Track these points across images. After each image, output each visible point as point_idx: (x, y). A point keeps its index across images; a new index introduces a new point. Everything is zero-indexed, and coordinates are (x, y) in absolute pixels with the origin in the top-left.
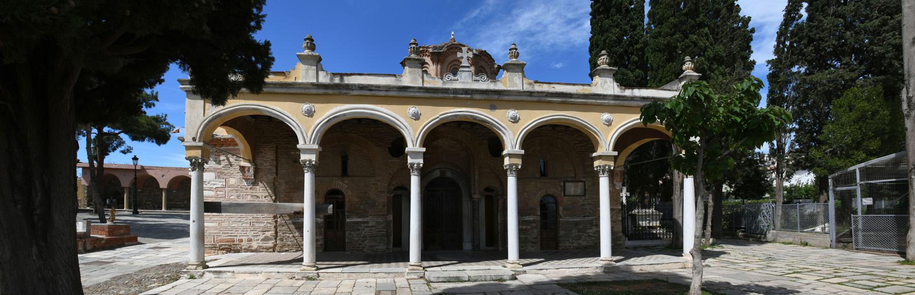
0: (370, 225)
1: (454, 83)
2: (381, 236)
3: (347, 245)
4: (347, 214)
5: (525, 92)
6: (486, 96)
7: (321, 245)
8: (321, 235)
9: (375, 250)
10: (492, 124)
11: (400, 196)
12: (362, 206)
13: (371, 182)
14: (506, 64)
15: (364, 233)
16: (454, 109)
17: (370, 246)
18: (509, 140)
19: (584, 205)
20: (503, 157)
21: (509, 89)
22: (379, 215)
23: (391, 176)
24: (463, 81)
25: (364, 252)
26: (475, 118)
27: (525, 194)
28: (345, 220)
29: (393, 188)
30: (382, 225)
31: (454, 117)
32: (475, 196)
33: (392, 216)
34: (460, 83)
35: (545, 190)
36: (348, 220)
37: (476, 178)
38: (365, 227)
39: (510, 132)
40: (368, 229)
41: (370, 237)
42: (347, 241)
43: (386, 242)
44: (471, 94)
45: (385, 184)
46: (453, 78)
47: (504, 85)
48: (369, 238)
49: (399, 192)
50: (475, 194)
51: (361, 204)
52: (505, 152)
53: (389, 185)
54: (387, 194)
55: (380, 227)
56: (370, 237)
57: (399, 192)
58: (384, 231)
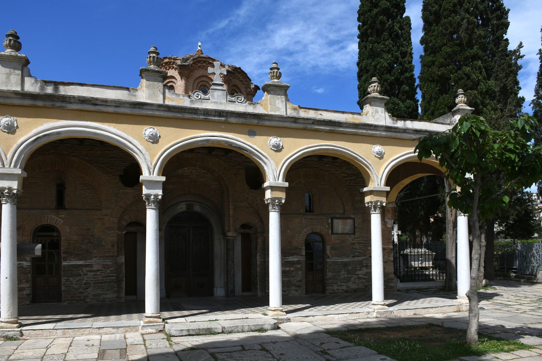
0: (95, 268)
1: (204, 102)
2: (109, 282)
3: (63, 294)
5: (289, 117)
6: (244, 120)
8: (27, 282)
10: (251, 152)
11: (135, 233)
14: (266, 84)
15: (86, 279)
16: (205, 132)
17: (94, 295)
18: (271, 171)
19: (354, 244)
20: (264, 190)
21: (270, 113)
22: (106, 256)
24: (216, 101)
26: (231, 144)
27: (289, 231)
29: (125, 224)
30: (110, 269)
31: (204, 143)
32: (230, 234)
34: (211, 102)
35: (310, 227)
36: (64, 263)
37: (231, 212)
38: (88, 271)
39: (272, 161)
40: (92, 274)
41: (94, 284)
43: (116, 289)
44: (226, 116)
46: (203, 96)
47: (264, 109)
48: (92, 285)
49: (132, 229)
50: (229, 231)
52: (266, 185)
55: (108, 271)
56: (94, 284)
57: (132, 229)
58: (113, 276)
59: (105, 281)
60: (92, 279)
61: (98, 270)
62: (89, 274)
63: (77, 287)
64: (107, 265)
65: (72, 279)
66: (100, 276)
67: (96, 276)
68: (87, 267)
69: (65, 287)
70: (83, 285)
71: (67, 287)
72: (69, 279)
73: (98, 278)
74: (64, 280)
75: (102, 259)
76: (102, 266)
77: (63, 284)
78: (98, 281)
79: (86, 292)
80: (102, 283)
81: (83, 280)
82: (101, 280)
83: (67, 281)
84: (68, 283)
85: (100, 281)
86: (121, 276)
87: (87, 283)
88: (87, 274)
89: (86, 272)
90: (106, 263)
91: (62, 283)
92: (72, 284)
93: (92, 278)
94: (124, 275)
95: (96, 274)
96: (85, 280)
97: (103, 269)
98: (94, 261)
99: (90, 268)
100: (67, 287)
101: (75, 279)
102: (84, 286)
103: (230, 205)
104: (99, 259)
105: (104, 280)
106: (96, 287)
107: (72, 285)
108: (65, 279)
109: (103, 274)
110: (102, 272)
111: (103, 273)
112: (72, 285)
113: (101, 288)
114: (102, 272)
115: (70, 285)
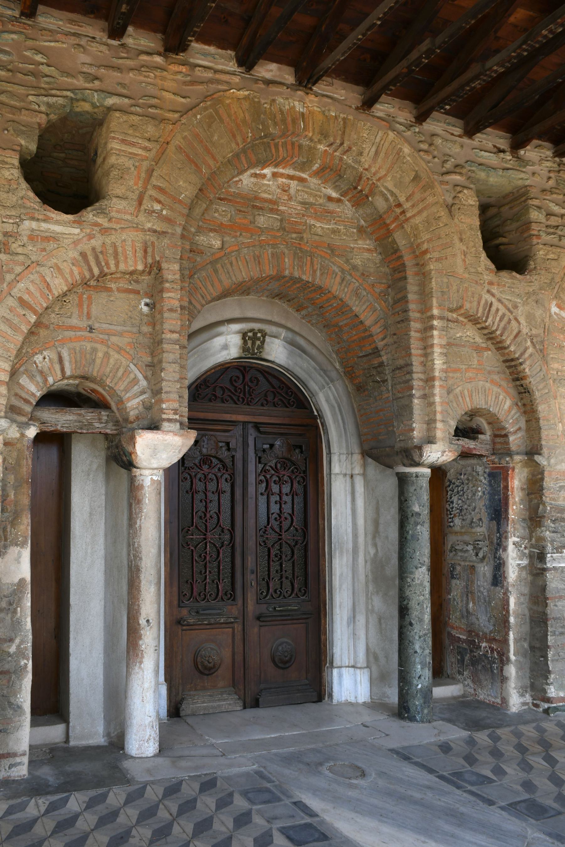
23: (33, 318)
33: (26, 554)
53: (14, 373)
86: (13, 649)
94: (30, 644)
103: (435, 333)
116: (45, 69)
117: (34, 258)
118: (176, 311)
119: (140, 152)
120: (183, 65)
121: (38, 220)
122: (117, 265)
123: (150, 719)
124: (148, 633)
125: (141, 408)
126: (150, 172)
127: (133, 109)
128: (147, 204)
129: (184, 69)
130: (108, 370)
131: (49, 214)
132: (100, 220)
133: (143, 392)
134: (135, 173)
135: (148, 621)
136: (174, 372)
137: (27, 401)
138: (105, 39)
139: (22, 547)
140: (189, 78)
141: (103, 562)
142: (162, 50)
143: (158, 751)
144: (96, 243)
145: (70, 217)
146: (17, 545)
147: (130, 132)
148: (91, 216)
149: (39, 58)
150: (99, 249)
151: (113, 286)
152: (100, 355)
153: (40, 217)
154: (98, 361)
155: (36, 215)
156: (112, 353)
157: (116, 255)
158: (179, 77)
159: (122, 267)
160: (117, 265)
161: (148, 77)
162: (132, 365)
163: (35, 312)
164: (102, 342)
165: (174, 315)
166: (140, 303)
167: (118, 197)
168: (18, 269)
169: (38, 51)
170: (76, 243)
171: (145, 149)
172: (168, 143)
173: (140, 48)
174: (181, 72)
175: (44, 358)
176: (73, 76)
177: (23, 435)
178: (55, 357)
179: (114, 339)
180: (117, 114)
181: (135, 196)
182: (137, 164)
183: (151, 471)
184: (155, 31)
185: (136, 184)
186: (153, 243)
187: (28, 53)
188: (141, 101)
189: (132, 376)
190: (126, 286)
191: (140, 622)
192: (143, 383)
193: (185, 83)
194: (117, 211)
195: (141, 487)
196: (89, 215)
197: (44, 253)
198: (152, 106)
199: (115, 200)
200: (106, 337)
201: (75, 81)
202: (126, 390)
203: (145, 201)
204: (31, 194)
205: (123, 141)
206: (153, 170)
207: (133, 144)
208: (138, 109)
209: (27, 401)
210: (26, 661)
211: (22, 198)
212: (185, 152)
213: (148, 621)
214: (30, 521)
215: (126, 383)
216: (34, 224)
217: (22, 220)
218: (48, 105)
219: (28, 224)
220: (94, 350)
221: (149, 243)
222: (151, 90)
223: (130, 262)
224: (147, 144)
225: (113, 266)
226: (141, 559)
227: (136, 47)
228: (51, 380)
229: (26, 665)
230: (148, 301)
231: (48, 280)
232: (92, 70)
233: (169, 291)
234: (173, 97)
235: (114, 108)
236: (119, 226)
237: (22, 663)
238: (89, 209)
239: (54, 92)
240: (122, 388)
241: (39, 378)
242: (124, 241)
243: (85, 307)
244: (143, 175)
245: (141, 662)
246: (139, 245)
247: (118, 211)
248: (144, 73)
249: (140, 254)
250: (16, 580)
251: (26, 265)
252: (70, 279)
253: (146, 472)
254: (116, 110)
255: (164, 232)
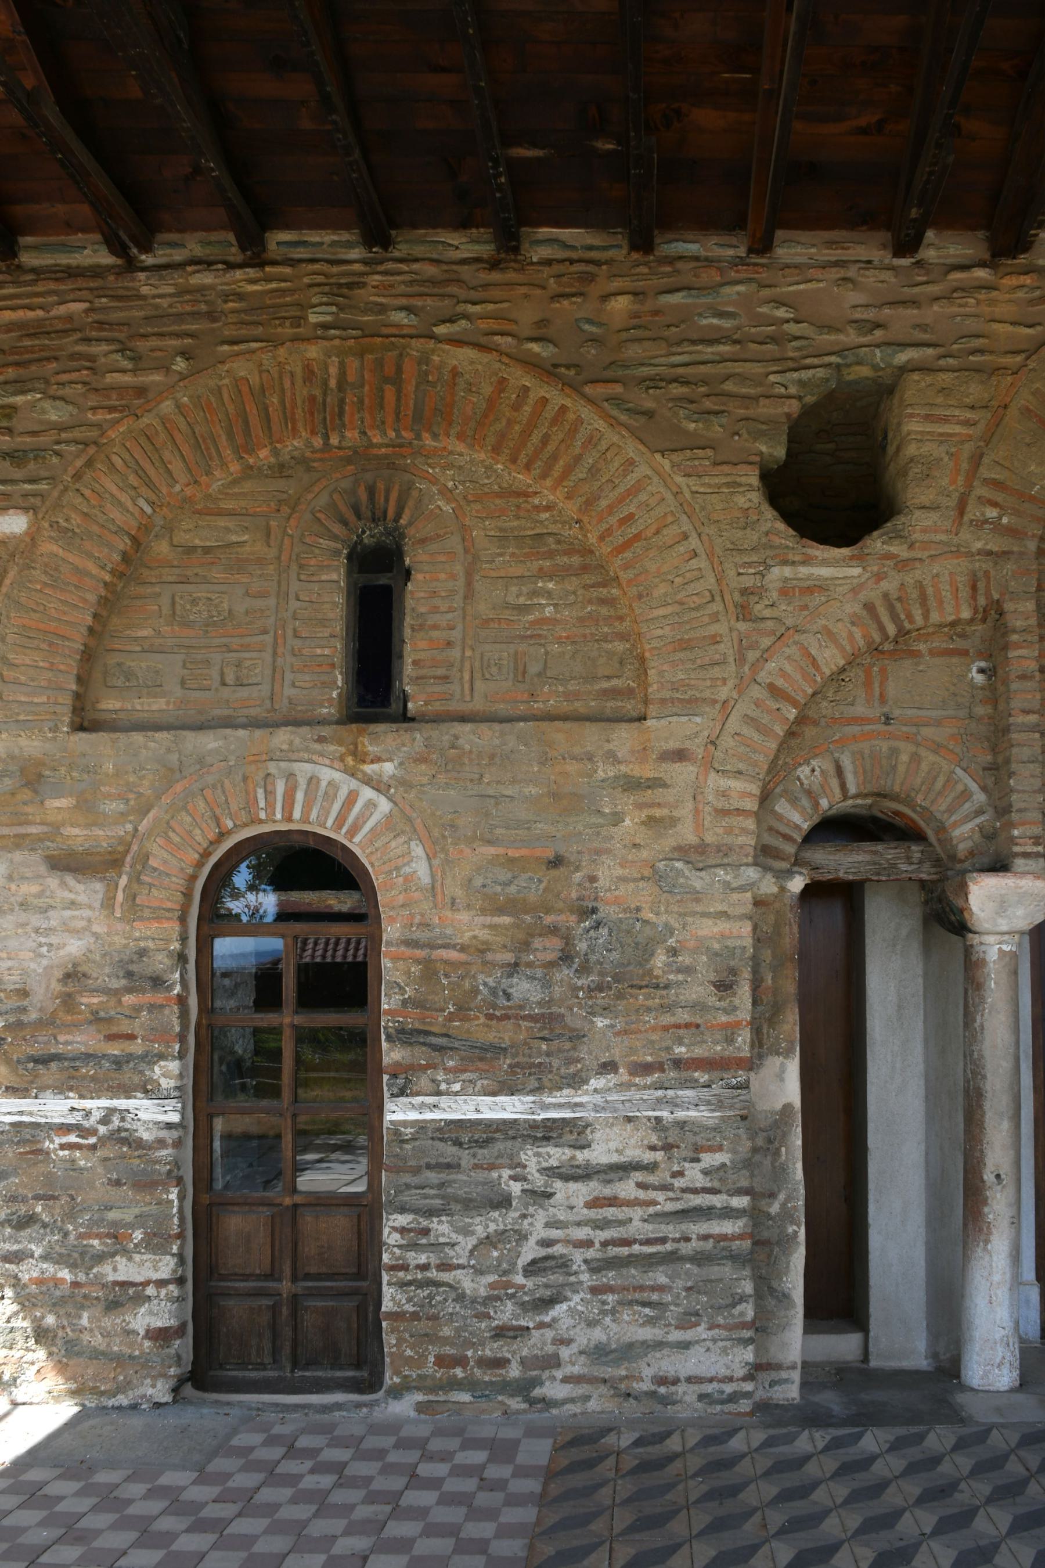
0: (600, 1154)
2: (700, 1259)
3: (389, 1340)
4: (392, 1054)
7: (160, 1336)
8: (155, 1243)
9: (646, 1386)
12: (523, 989)
13: (604, 771)
15: (539, 1231)
17: (599, 1353)
22: (678, 1063)
23: (792, 713)
25: (547, 1403)
28: (380, 1110)
30: (709, 1160)
33: (793, 1068)
38: (551, 1172)
40: (580, 1192)
41: (595, 1267)
42: (391, 1298)
43: (748, 1311)
45: (737, 785)
48: (585, 1277)
51: (514, 968)
53: (765, 798)
54: (752, 873)
55: (694, 1175)
58: (728, 1213)
59: (669, 1247)
60: (582, 1233)
61: (624, 1169)
62: (559, 1197)
63: (483, 1292)
64: (682, 1125)
65: (445, 1228)
66: (637, 1213)
67: (610, 1212)
68: (546, 1138)
69: (403, 1285)
70: (519, 1279)
71: (421, 1284)
72: (426, 1232)
73: (621, 1223)
74: (396, 1236)
75: (649, 1080)
76: (654, 1139)
77: (393, 1268)
78: (625, 1251)
79: (541, 1325)
80: (649, 1262)
81: (522, 1237)
82: (648, 1242)
83: (413, 1246)
84: (423, 1259)
85: (636, 1248)
86: (775, 1208)
87: (546, 1258)
88: (550, 1195)
89: (539, 1181)
90: (680, 1114)
91: (386, 1258)
92: (445, 1266)
93: (579, 1224)
94: (801, 1203)
95: (607, 1191)
96: (532, 1241)
97: (659, 1155)
98: (598, 1099)
99: (568, 1152)
100: (421, 1284)
101: (466, 1231)
102: (529, 1283)
104: (622, 1086)
105: (663, 1240)
106: (609, 1289)
107: (446, 1277)
108: (402, 1231)
109: (660, 1196)
110: (652, 1179)
111: (655, 1188)
112: (446, 1277)
113: (645, 1304)
114: (652, 1179)
115: (433, 1274)
116: (792, 328)
117: (789, 622)
118: (1031, 678)
119: (958, 429)
120: (1026, 273)
121: (793, 563)
122: (926, 616)
123: (1003, 1332)
124: (998, 1195)
125: (977, 836)
126: (976, 460)
127: (942, 362)
128: (973, 512)
129: (1027, 280)
130: (919, 781)
131: (809, 551)
132: (894, 549)
133: (979, 812)
134: (952, 464)
135: (998, 1176)
136: (1032, 776)
137: (787, 838)
138: (888, 259)
139: (787, 1057)
140: (1038, 293)
141: (922, 1083)
142: (987, 256)
143: (1017, 1383)
144: (889, 585)
145: (845, 551)
146: (778, 1054)
147: (939, 400)
148: (879, 544)
149: (782, 313)
150: (894, 595)
151: (922, 647)
152: (904, 758)
153: (797, 558)
154: (901, 769)
155: (791, 557)
156: (923, 752)
157: (923, 599)
158: (1020, 294)
159: (935, 617)
160: (926, 616)
161: (965, 305)
162: (958, 770)
163: (794, 703)
164: (907, 738)
165: (1029, 685)
166: (970, 670)
167: (923, 507)
168: (766, 642)
169: (780, 303)
170: (855, 590)
171: (967, 423)
172: (1006, 407)
173: (949, 261)
174: (1022, 286)
175: (813, 771)
176: (838, 330)
177: (783, 889)
178: (830, 768)
179: (926, 731)
180: (916, 376)
181: (953, 503)
182: (953, 450)
183: (998, 937)
184: (973, 228)
185: (953, 482)
186: (986, 573)
187: (764, 309)
188: (955, 346)
189: (960, 787)
190: (944, 645)
191: (985, 1177)
192: (980, 797)
193: (1031, 302)
194: (922, 531)
195: (982, 963)
196: (876, 543)
197: (806, 613)
198: (974, 352)
199: (918, 513)
200: (914, 729)
201: (842, 337)
202: (951, 811)
203: (969, 508)
204: (781, 526)
205: (928, 418)
206: (982, 455)
207: (945, 420)
208: (950, 361)
209: (787, 838)
210: (795, 1228)
211: (767, 534)
212: (1036, 416)
213: (998, 1176)
214: (797, 1017)
215: (949, 799)
216: (787, 571)
217: (768, 567)
218: (801, 383)
219: (776, 572)
220: (894, 752)
221: (980, 574)
222: (973, 325)
223: (949, 608)
224: (969, 415)
225: (919, 621)
226: (984, 1077)
227: (942, 261)
228: (824, 803)
229: (796, 1232)
230: (983, 664)
231: (813, 652)
232: (870, 314)
233: (1018, 646)
234: (1010, 328)
235: (910, 367)
236: (927, 554)
237: (790, 1230)
238: (875, 534)
239: (808, 361)
240: (943, 807)
241: (805, 802)
242: (937, 575)
243: (876, 685)
244: (965, 466)
245: (987, 1242)
246: (962, 580)
247: (924, 531)
248: (958, 301)
249: (964, 593)
250: (778, 1106)
251: (778, 634)
252: (848, 648)
253: (990, 939)
254: (913, 370)
255: (1004, 553)
